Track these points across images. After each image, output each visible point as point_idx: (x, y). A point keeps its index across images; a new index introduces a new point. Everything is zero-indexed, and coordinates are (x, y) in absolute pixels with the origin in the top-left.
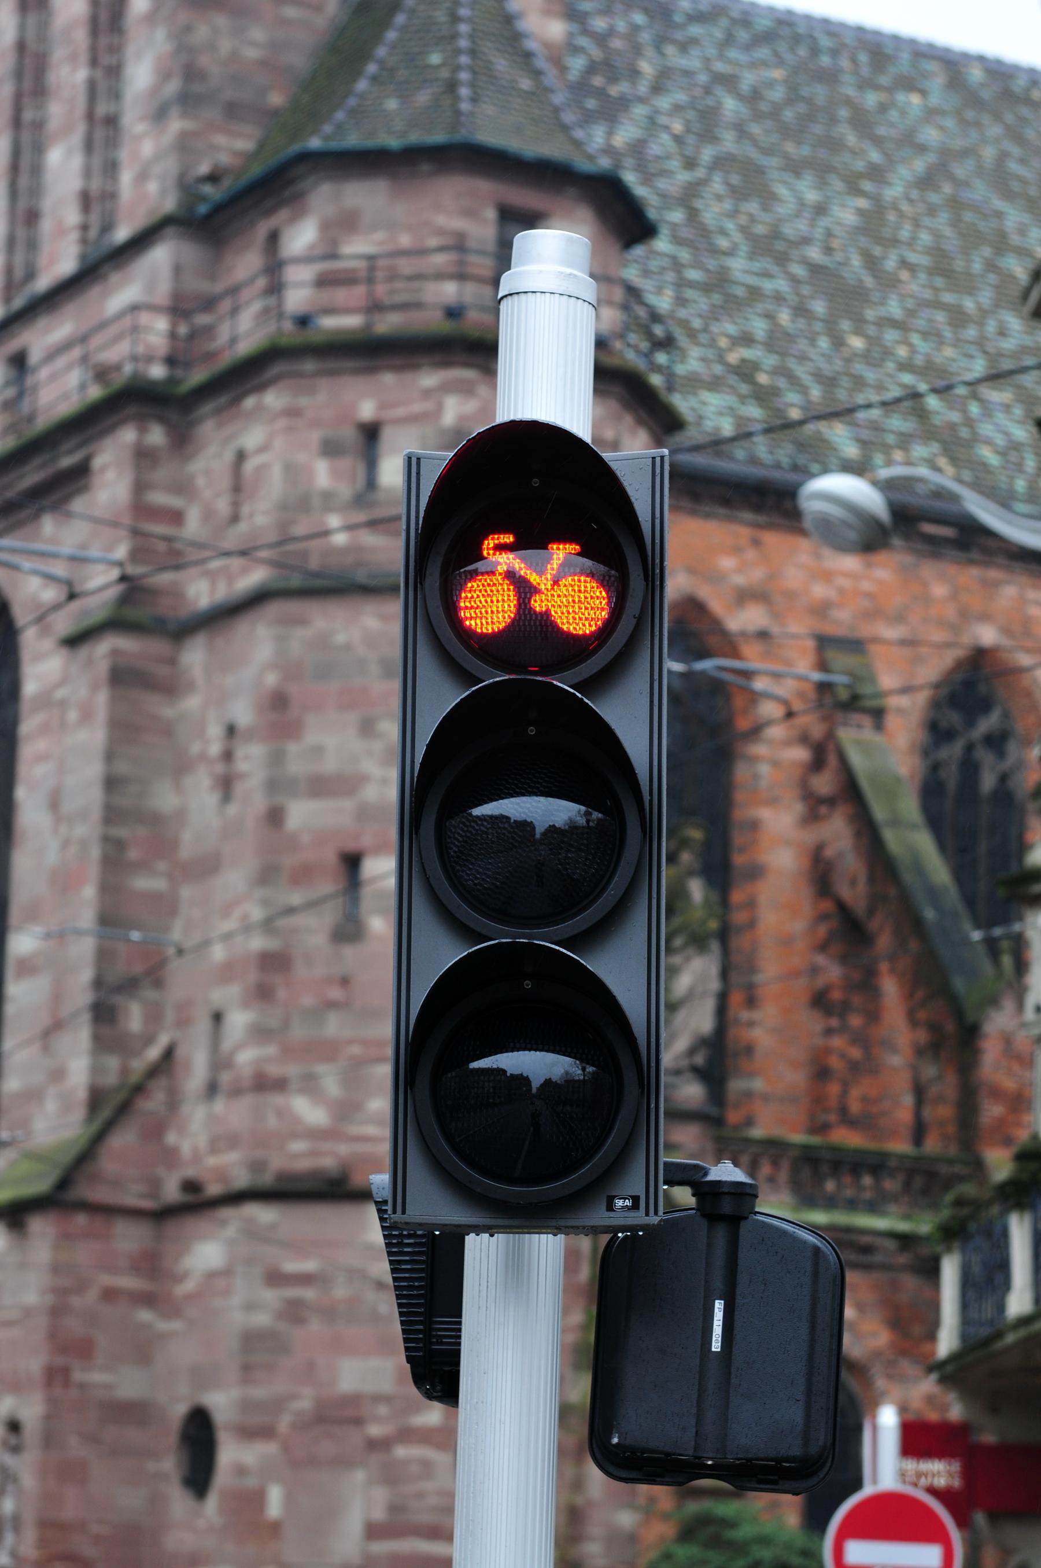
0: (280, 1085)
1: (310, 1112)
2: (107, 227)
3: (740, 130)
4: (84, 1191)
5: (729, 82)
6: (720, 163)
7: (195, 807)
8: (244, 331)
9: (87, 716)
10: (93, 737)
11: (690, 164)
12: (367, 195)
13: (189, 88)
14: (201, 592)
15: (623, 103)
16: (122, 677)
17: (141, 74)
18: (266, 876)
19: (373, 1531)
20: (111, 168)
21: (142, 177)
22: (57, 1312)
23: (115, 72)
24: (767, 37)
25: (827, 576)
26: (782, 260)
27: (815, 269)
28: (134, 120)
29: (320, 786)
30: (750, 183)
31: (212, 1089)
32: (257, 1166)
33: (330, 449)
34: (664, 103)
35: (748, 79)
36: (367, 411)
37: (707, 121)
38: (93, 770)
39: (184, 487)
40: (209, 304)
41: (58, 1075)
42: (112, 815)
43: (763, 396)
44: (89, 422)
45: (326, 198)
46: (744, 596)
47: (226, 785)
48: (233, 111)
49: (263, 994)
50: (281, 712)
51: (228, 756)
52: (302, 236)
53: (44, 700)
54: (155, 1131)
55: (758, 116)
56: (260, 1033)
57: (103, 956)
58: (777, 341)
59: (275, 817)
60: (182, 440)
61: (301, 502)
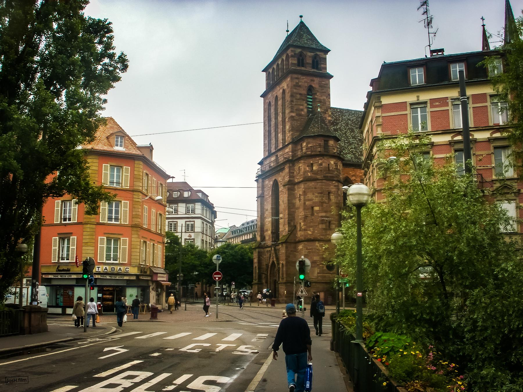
0: (307, 230)
1: (310, 233)
2: (285, 142)
3: (351, 125)
4: (288, 241)
5: (349, 119)
6: (348, 129)
7: (297, 202)
8: (299, 153)
9: (286, 193)
10: (286, 195)
11: (345, 129)
12: (310, 140)
13: (292, 129)
14: (296, 181)
15: (338, 123)
16: (289, 189)
17: (287, 127)
18: (304, 209)
19: (318, 273)
20: (285, 137)
21: (288, 138)
22: (286, 253)
23: (285, 126)
24: (354, 114)
25: (361, 173)
26: (356, 139)
27: (359, 139)
28: (287, 132)
29: (309, 200)
30: (352, 131)
31: (300, 230)
32: (305, 238)
33: (308, 166)
34: (342, 123)
35: (352, 119)
36: (312, 162)
37: (347, 124)
38: (287, 199)
39: (294, 170)
40: (296, 151)
41: (285, 229)
42: (289, 203)
43: (354, 154)
44: (284, 163)
45: (306, 141)
46: (353, 176)
47: (300, 200)
48: (297, 131)
49: (304, 221)
50: (305, 193)
51: (300, 197)
52: (304, 144)
53: (282, 191)
54: (295, 235)
55: (353, 123)
56: (304, 225)
57: (289, 218)
58: (355, 148)
59: (305, 203)
60: (294, 165)
61: (305, 172)
